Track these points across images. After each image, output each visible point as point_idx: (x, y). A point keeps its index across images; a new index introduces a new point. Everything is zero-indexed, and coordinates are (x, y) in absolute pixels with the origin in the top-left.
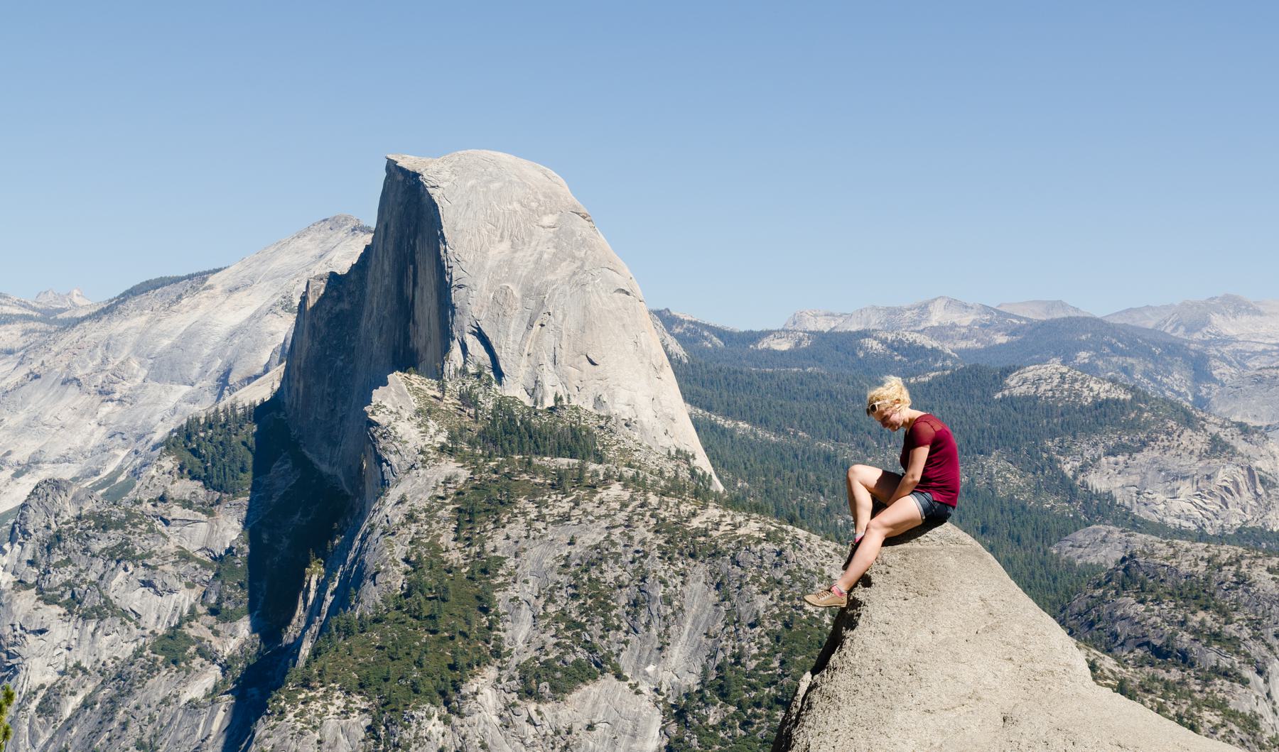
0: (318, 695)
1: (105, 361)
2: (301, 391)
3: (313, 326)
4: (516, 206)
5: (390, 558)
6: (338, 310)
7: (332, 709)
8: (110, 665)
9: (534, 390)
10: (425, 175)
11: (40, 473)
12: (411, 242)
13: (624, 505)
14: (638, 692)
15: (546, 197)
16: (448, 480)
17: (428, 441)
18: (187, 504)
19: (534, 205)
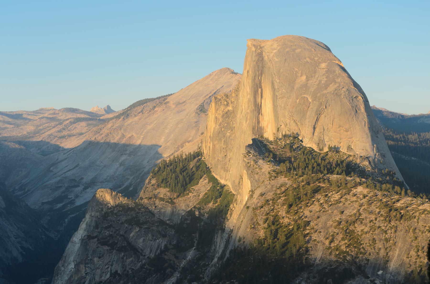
2: (211, 147)
3: (216, 118)
4: (308, 59)
5: (256, 222)
6: (227, 110)
8: (130, 272)
10: (265, 47)
12: (260, 78)
13: (365, 197)
15: (321, 55)
16: (282, 186)
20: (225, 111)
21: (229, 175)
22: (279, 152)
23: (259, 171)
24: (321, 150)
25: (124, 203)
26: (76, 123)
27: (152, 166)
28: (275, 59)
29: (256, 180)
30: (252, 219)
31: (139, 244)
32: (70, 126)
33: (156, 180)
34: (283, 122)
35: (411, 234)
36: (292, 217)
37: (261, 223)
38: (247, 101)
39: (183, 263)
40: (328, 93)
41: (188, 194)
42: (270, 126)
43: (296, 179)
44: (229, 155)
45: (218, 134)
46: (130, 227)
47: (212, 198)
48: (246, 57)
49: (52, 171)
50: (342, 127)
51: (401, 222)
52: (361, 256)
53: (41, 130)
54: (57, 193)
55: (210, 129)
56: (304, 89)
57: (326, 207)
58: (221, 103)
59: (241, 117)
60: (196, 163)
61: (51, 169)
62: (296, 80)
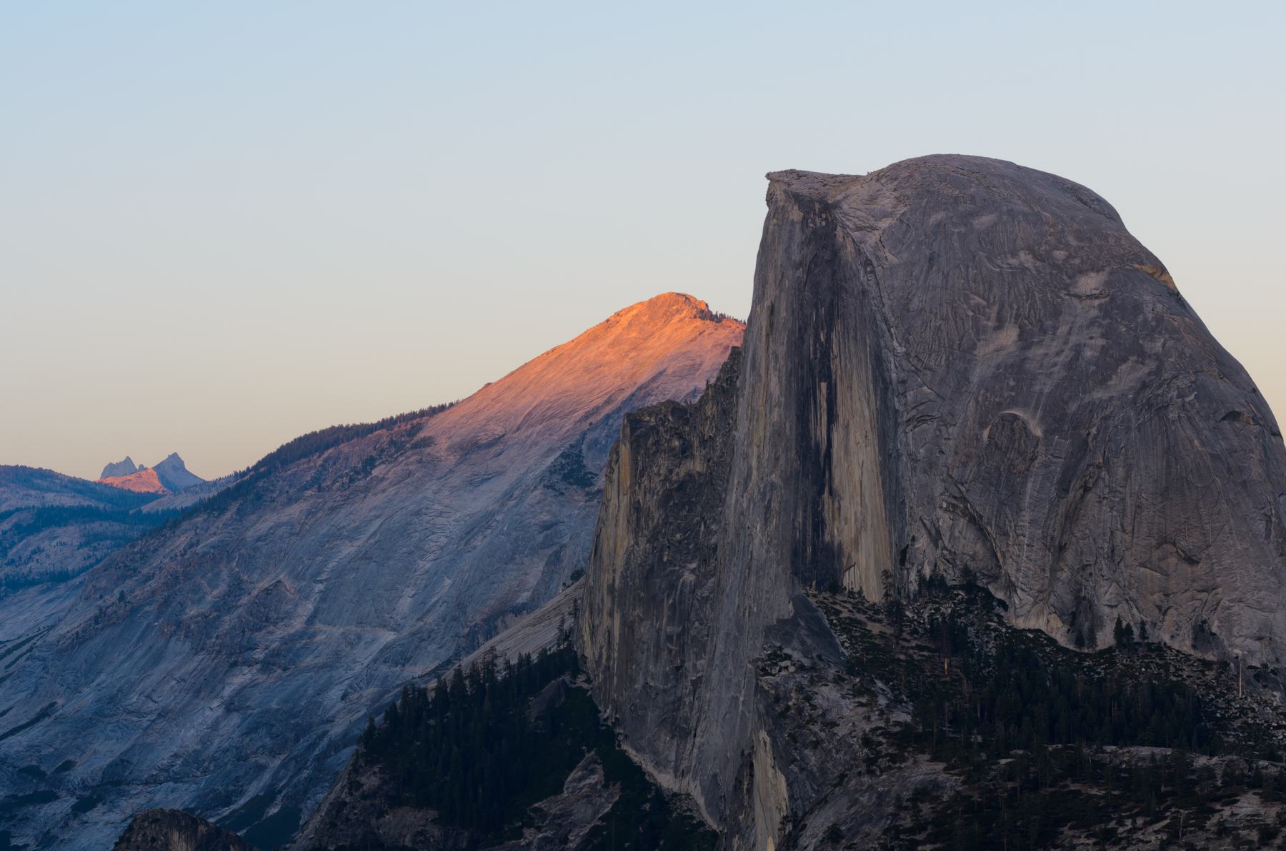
1: (237, 587)
2: (616, 633)
3: (636, 508)
4: (1025, 258)
6: (682, 474)
10: (845, 207)
11: (123, 803)
15: (1080, 239)
17: (877, 722)
19: (1060, 255)
20: (675, 478)
21: (695, 751)
22: (906, 654)
23: (822, 735)
24: (1079, 642)
27: (360, 714)
28: (887, 254)
29: (811, 772)
32: (14, 544)
34: (924, 524)
38: (768, 434)
40: (1111, 398)
42: (866, 541)
44: (695, 665)
50: (1174, 544)
55: (609, 554)
56: (1012, 383)
58: (657, 443)
59: (745, 505)
62: (975, 344)
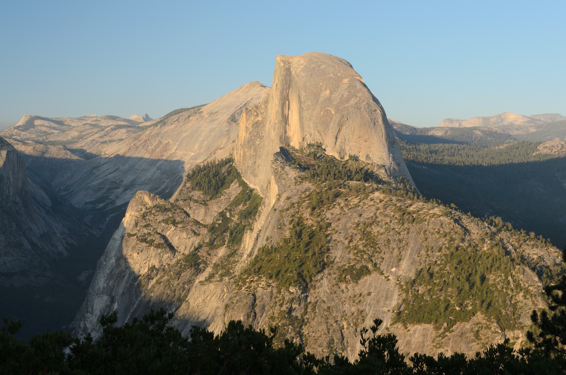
0: (255, 280)
3: (247, 127)
4: (332, 75)
5: (283, 223)
7: (260, 286)
8: (167, 267)
9: (342, 152)
10: (293, 63)
12: (287, 91)
13: (381, 201)
14: (389, 280)
15: (344, 71)
16: (306, 190)
18: (196, 201)
20: (255, 121)
23: (285, 177)
24: (342, 158)
25: (161, 204)
26: (116, 130)
29: (283, 185)
30: (279, 221)
31: (174, 242)
33: (191, 183)
35: (422, 235)
36: (315, 219)
37: (287, 224)
39: (215, 260)
40: (349, 106)
41: (220, 197)
42: (296, 136)
43: (319, 184)
45: (248, 142)
46: (167, 226)
47: (242, 201)
48: (275, 71)
49: (94, 174)
51: (414, 224)
52: (376, 254)
53: (84, 135)
54: (99, 194)
56: (328, 102)
57: (346, 211)
58: (251, 113)
60: (228, 168)
61: (93, 172)
